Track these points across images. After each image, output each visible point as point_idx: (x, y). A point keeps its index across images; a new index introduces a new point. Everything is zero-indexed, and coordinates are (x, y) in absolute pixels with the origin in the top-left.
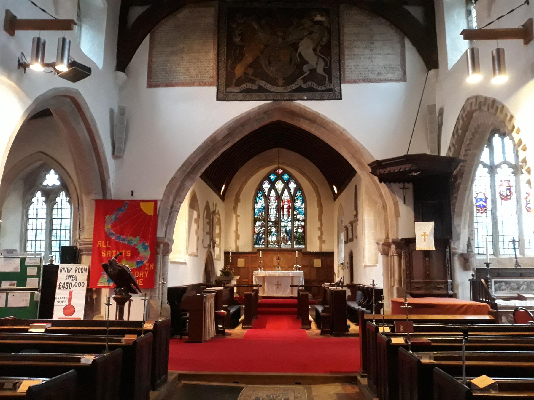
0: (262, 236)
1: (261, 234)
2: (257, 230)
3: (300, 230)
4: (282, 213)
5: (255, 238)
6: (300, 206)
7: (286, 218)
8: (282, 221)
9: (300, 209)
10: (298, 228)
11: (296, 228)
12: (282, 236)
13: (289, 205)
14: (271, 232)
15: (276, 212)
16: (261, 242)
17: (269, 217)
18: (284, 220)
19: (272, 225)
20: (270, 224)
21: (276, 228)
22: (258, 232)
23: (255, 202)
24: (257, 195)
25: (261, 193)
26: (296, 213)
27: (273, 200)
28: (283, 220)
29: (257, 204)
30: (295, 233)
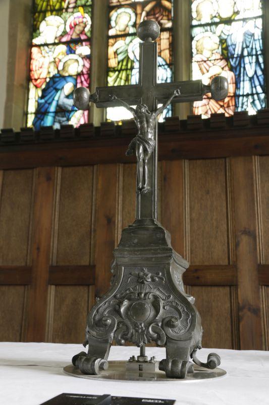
5: (32, 107)
22: (54, 72)
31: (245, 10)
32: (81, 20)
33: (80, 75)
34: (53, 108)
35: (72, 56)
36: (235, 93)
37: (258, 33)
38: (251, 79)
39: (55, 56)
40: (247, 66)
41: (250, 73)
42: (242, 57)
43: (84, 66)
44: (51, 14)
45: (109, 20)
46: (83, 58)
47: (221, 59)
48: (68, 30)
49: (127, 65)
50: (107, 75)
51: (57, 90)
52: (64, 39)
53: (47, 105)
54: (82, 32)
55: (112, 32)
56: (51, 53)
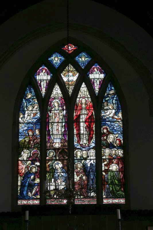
0: (34, 179)
1: (32, 177)
2: (23, 168)
3: (114, 167)
4: (75, 131)
6: (113, 117)
7: (84, 141)
8: (76, 149)
9: (114, 122)
10: (111, 161)
11: (106, 163)
12: (77, 178)
13: (90, 114)
14: (53, 170)
15: (63, 130)
16: (31, 193)
17: (49, 140)
18: (81, 145)
19: (55, 156)
20: (51, 154)
21: (63, 163)
23: (19, 109)
24: (24, 96)
25: (33, 91)
26: (105, 131)
27: (56, 105)
28: (79, 147)
29: (24, 114)
30: (104, 173)
31: (91, 156)
32: (36, 152)
33: (36, 172)
34: (27, 185)
35: (33, 166)
36: (87, 184)
37: (94, 164)
38: (92, 180)
39: (27, 165)
40: (91, 175)
41: (92, 178)
42: (89, 172)
43: (38, 169)
44: (25, 149)
45: (47, 153)
46: (37, 167)
47: (83, 172)
48: (32, 155)
49: (53, 171)
50: (46, 174)
51: (28, 178)
52: (30, 159)
53: (25, 183)
54: (37, 157)
55: (47, 158)
56: (25, 164)
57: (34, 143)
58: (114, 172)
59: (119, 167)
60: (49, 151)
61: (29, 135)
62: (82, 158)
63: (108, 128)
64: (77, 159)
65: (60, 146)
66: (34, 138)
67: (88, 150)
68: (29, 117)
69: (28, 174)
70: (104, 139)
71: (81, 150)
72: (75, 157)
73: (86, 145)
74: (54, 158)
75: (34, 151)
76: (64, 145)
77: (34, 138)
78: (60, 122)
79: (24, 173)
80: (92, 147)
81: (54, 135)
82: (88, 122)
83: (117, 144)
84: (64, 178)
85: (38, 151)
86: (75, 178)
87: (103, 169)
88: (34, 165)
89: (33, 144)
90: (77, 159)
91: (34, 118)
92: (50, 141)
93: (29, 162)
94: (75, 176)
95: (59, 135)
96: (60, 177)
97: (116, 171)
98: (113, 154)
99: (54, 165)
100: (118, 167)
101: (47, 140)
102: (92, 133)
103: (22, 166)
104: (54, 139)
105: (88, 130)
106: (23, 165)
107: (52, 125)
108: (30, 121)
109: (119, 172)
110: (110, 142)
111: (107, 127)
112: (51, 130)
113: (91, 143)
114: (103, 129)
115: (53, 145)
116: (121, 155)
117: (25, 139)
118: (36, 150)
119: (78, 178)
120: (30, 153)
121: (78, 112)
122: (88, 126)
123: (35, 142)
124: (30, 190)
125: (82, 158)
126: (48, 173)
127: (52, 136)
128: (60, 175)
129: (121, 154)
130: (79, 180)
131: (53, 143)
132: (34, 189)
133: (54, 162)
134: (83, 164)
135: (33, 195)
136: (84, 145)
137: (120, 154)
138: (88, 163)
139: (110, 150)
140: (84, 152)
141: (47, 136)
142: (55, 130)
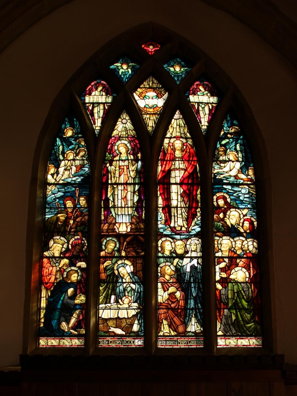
0: (74, 297)
1: (70, 291)
4: (160, 201)
7: (179, 222)
10: (233, 261)
11: (223, 265)
12: (162, 296)
15: (136, 199)
16: (68, 323)
17: (106, 217)
18: (173, 229)
19: (119, 251)
26: (221, 202)
28: (168, 232)
30: (219, 286)
31: (192, 251)
35: (73, 268)
39: (60, 266)
41: (194, 295)
42: (189, 282)
49: (113, 279)
52: (67, 255)
57: (76, 223)
58: (240, 283)
59: (250, 274)
60: (106, 239)
61: (65, 207)
62: (174, 255)
63: (227, 197)
64: (163, 257)
65: (129, 230)
66: (75, 213)
67: (187, 239)
68: (67, 173)
69: (62, 286)
70: (219, 218)
71: (173, 238)
72: (160, 252)
73: (184, 229)
74: (116, 254)
75: (75, 239)
76: (136, 228)
77: (75, 213)
78: (130, 184)
79: (54, 283)
80: (193, 232)
81: (118, 207)
82: (187, 184)
83: (245, 228)
84: (136, 293)
85: (84, 239)
86: (159, 294)
87: (218, 278)
88: (75, 266)
89: (74, 226)
90: (163, 257)
91: (77, 174)
92: (109, 221)
93: (66, 261)
94: (160, 291)
95: (128, 207)
96: (128, 293)
97: (243, 283)
98: (236, 248)
99: (115, 268)
100: (247, 273)
101: (103, 218)
102: (194, 205)
103: (51, 268)
104: (117, 216)
105: (186, 200)
106: (53, 267)
107: (114, 188)
108: (69, 180)
109: (250, 283)
110: (232, 225)
111: (225, 195)
112: (111, 199)
113: (193, 224)
114: (217, 199)
115: (115, 227)
116: (254, 251)
117: (59, 215)
118: (79, 237)
119: (166, 295)
120: (68, 242)
121: (166, 165)
122: (187, 192)
123: (78, 222)
124: (65, 317)
125: (174, 255)
126: (102, 284)
127: (112, 210)
128: (129, 289)
129: (254, 249)
130: (168, 299)
131: (115, 224)
132: (74, 315)
133: (116, 262)
134: (176, 267)
135: (73, 328)
136: (179, 228)
137: (251, 248)
138: (187, 264)
139: (232, 240)
140: (179, 243)
141: (103, 209)
142: (120, 198)
